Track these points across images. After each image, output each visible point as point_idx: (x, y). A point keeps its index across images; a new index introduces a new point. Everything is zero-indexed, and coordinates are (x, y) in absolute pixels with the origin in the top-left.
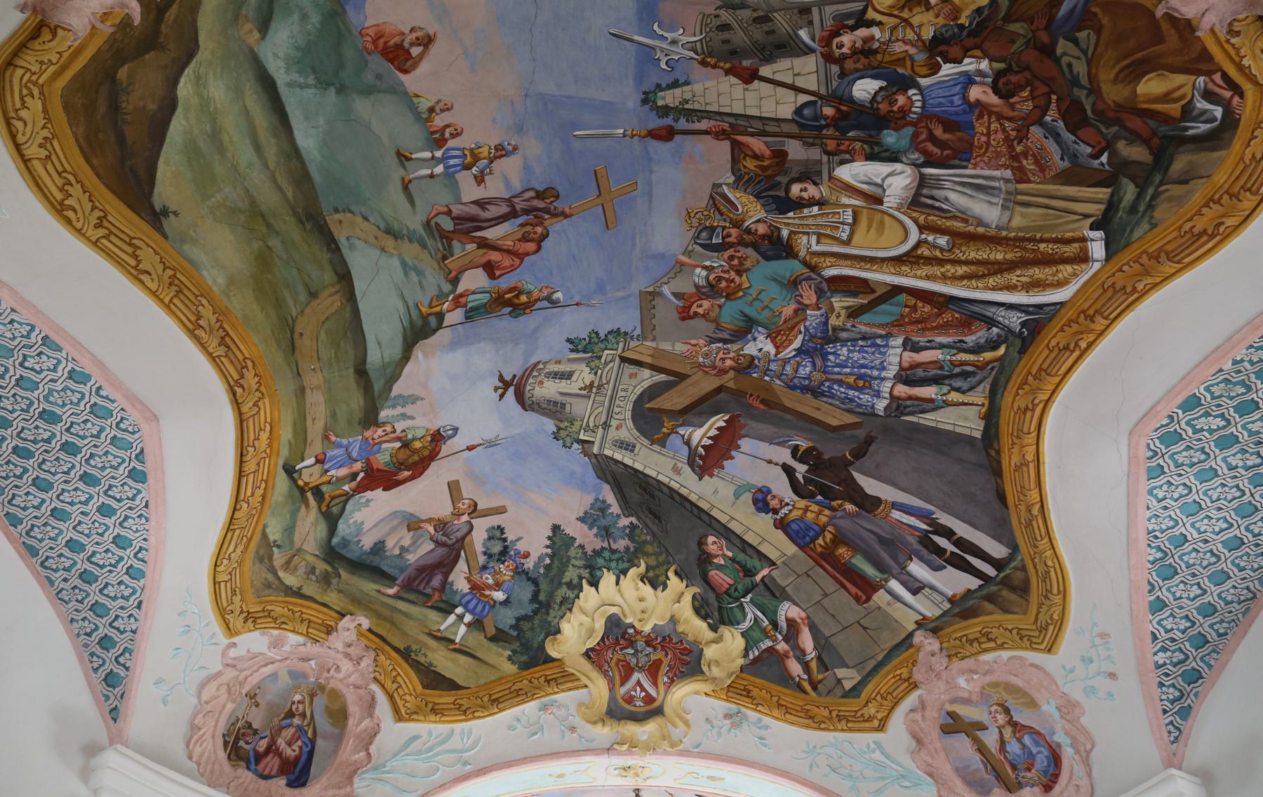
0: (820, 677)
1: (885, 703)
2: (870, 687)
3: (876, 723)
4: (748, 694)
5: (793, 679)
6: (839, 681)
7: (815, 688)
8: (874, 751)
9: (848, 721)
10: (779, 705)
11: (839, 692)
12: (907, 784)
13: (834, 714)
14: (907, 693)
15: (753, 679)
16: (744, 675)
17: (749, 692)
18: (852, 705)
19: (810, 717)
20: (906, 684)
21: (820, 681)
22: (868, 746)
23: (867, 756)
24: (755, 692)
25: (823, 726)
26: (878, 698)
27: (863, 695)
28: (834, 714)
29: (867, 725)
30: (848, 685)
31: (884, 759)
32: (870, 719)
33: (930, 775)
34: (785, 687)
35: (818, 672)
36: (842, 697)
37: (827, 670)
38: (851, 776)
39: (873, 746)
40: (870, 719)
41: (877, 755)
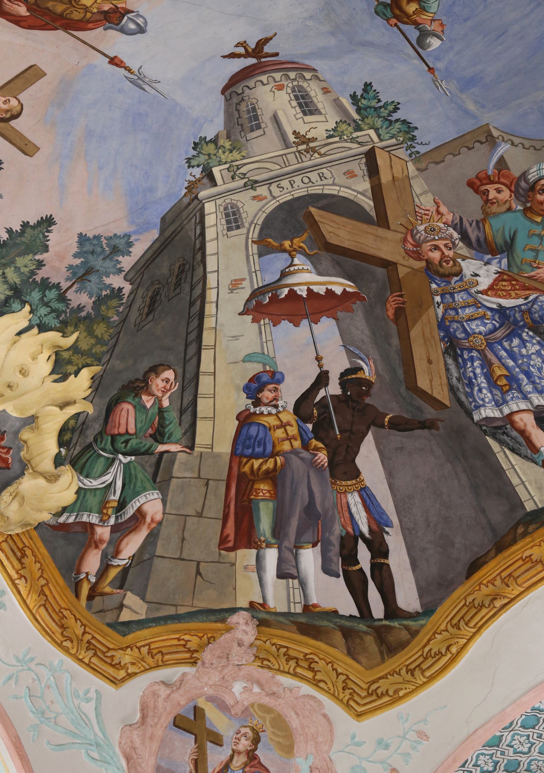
0: (108, 589)
1: (149, 660)
2: (145, 632)
3: (122, 674)
4: (20, 556)
5: (79, 572)
6: (121, 607)
7: (90, 598)
8: (88, 701)
9: (95, 654)
10: (42, 593)
11: (110, 617)
12: (95, 755)
13: (87, 637)
14: (179, 662)
15: (40, 544)
16: (35, 534)
17: (24, 555)
18: (113, 639)
19: (62, 626)
20: (188, 655)
21: (103, 594)
22: (87, 692)
23: (77, 702)
24: (29, 560)
25: (67, 644)
26: (145, 650)
27: (130, 637)
28: (87, 637)
29: (111, 671)
30: (125, 616)
31: (92, 715)
32: (117, 666)
33: (128, 759)
34: (63, 576)
35: (111, 584)
36: (109, 625)
37: (121, 587)
38: (43, 713)
39: (92, 694)
40: (117, 666)
41: (89, 708)
